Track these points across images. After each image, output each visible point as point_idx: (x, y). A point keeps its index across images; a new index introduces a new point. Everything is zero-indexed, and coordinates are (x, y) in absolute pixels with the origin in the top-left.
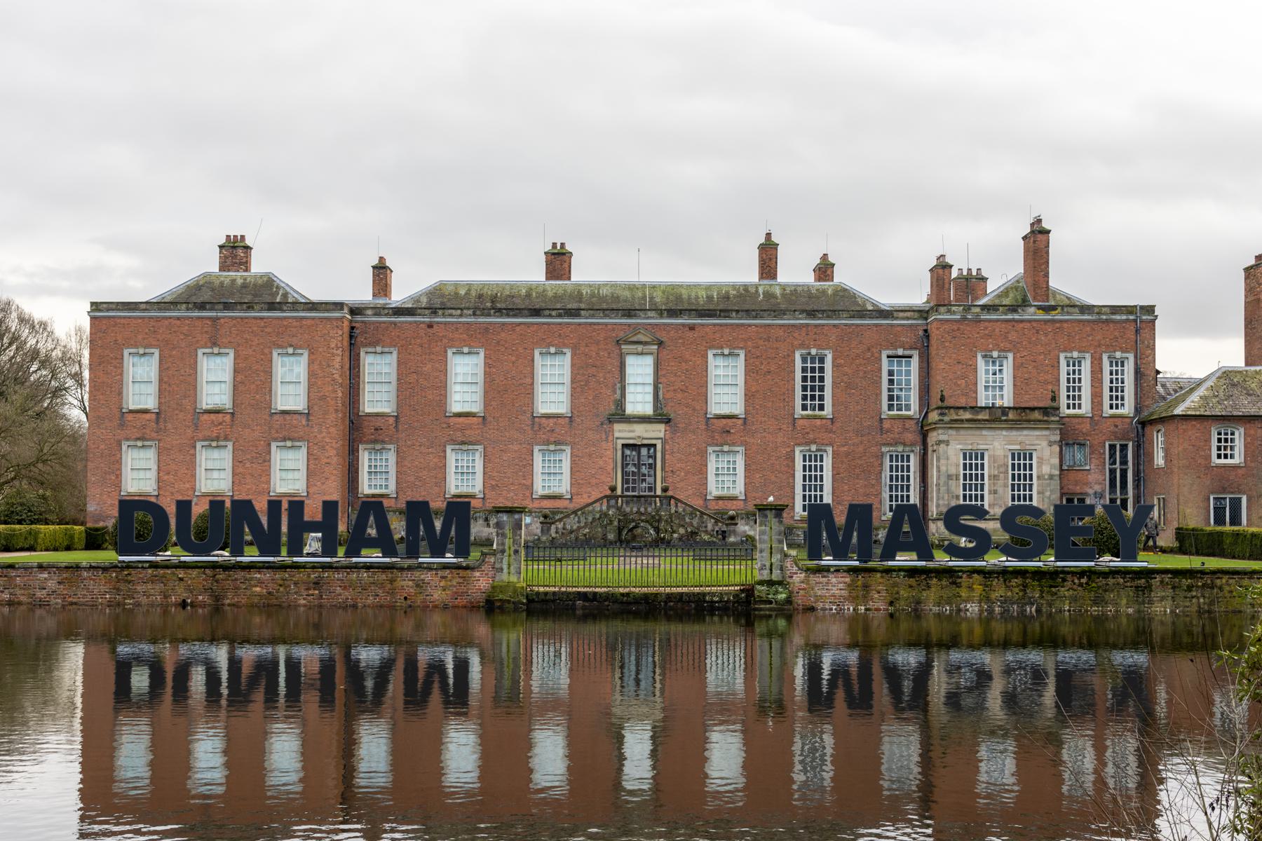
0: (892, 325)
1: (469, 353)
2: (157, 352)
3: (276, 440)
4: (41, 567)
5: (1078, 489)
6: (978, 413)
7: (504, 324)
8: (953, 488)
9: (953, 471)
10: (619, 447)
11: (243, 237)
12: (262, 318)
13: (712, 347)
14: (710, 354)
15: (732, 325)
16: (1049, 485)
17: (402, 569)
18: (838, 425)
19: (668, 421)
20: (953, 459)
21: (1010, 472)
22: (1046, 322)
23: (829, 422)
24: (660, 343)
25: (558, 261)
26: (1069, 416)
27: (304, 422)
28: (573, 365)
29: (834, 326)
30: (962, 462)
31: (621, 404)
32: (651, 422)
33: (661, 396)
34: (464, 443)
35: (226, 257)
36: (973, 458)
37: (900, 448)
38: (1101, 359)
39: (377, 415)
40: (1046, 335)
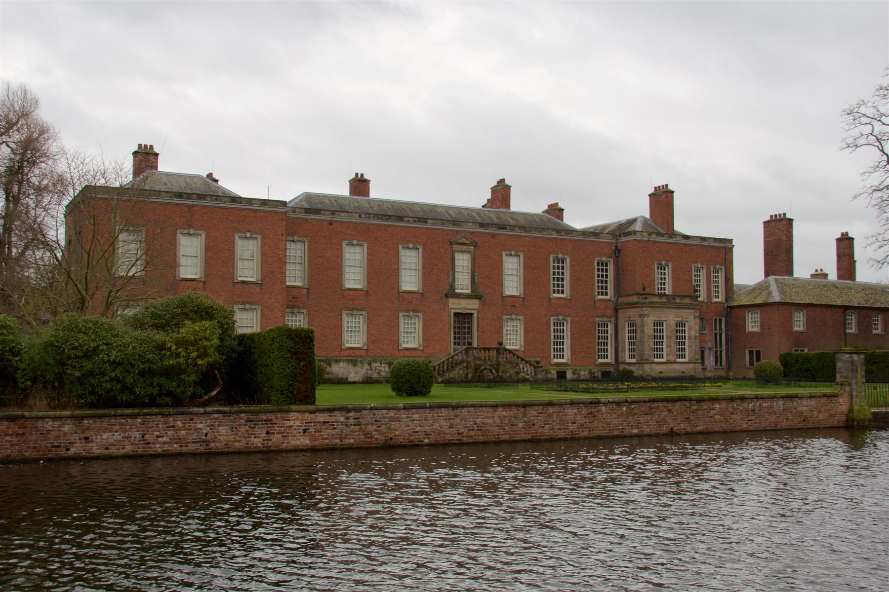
1: (357, 245)
3: (237, 303)
4: (573, 403)
7: (379, 225)
10: (452, 314)
11: (151, 147)
12: (226, 208)
13: (504, 250)
14: (504, 253)
17: (801, 398)
19: (479, 298)
22: (686, 245)
25: (360, 185)
27: (258, 291)
28: (423, 257)
29: (571, 240)
31: (452, 287)
34: (353, 309)
35: (141, 161)
36: (658, 323)
37: (605, 319)
39: (295, 287)
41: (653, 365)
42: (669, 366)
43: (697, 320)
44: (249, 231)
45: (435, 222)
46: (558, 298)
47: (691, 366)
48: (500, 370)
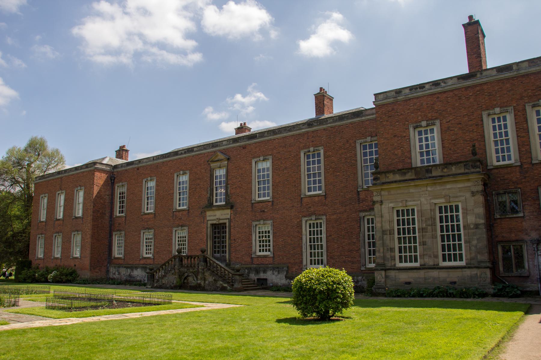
0: (363, 121)
2: (47, 195)
5: (513, 236)
6: (405, 174)
8: (388, 242)
9: (387, 227)
10: (209, 225)
13: (254, 158)
19: (232, 207)
21: (438, 224)
22: (467, 88)
24: (228, 159)
26: (497, 168)
30: (396, 218)
38: (524, 110)
41: (392, 273)
42: (422, 274)
43: (480, 198)
44: (80, 186)
45: (199, 148)
46: (310, 196)
47: (468, 272)
48: (199, 277)
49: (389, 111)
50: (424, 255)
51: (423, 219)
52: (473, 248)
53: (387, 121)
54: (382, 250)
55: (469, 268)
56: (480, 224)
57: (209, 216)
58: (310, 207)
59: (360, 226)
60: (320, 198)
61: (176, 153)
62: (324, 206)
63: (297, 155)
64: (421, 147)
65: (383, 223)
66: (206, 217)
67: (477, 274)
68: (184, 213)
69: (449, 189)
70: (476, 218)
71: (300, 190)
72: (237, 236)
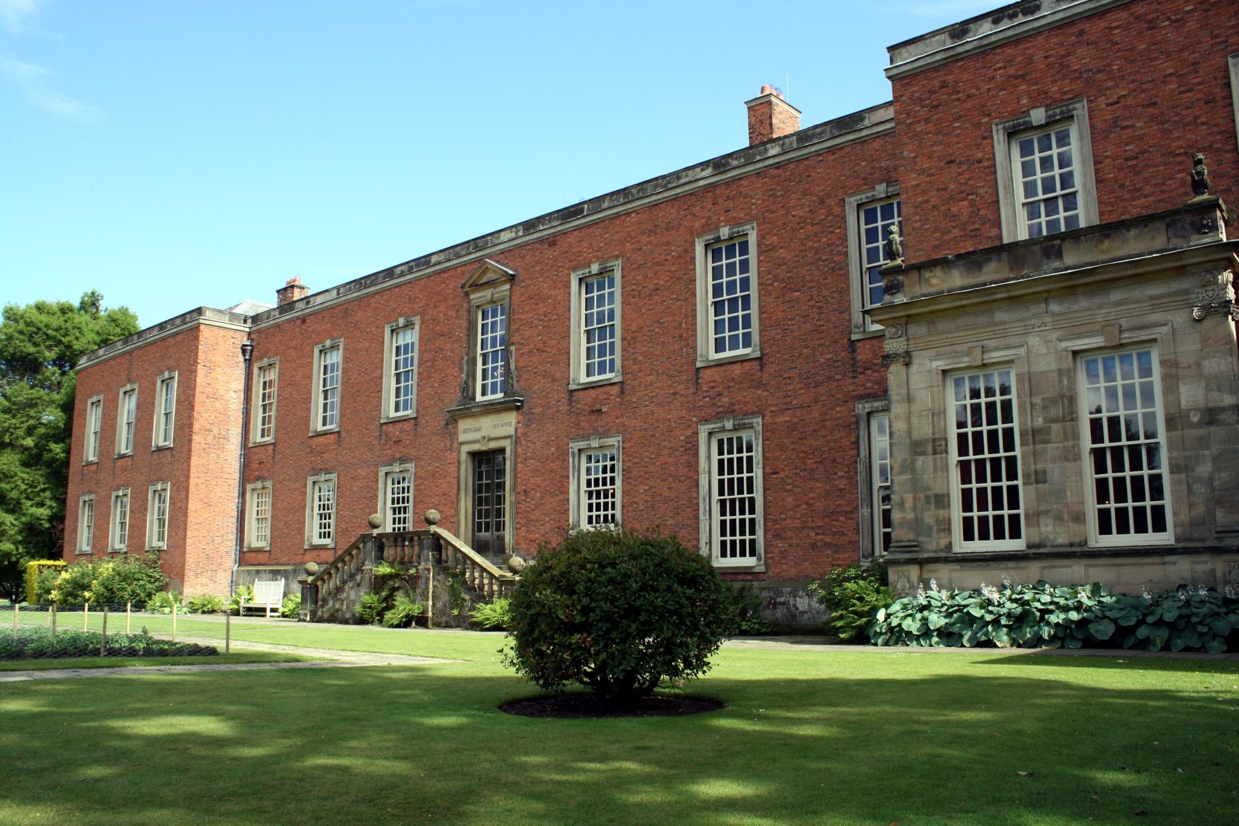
0: (862, 142)
8: (927, 478)
10: (464, 456)
13: (575, 269)
15: (602, 220)
16: (1203, 442)
18: (771, 369)
20: (924, 399)
23: (756, 364)
32: (498, 411)
33: (512, 367)
40: (1178, 24)
46: (720, 364)
47: (1182, 568)
49: (931, 92)
50: (1039, 514)
51: (1038, 400)
52: (1199, 489)
53: (927, 121)
54: (909, 503)
55: (1187, 552)
56: (1222, 410)
57: (465, 431)
58: (720, 395)
59: (857, 442)
60: (747, 365)
61: (389, 272)
62: (758, 388)
63: (686, 251)
64: (1029, 189)
65: (914, 420)
66: (456, 433)
67: (1213, 572)
68: (407, 426)
69: (1119, 304)
70: (1208, 389)
71: (694, 348)
72: (533, 480)
